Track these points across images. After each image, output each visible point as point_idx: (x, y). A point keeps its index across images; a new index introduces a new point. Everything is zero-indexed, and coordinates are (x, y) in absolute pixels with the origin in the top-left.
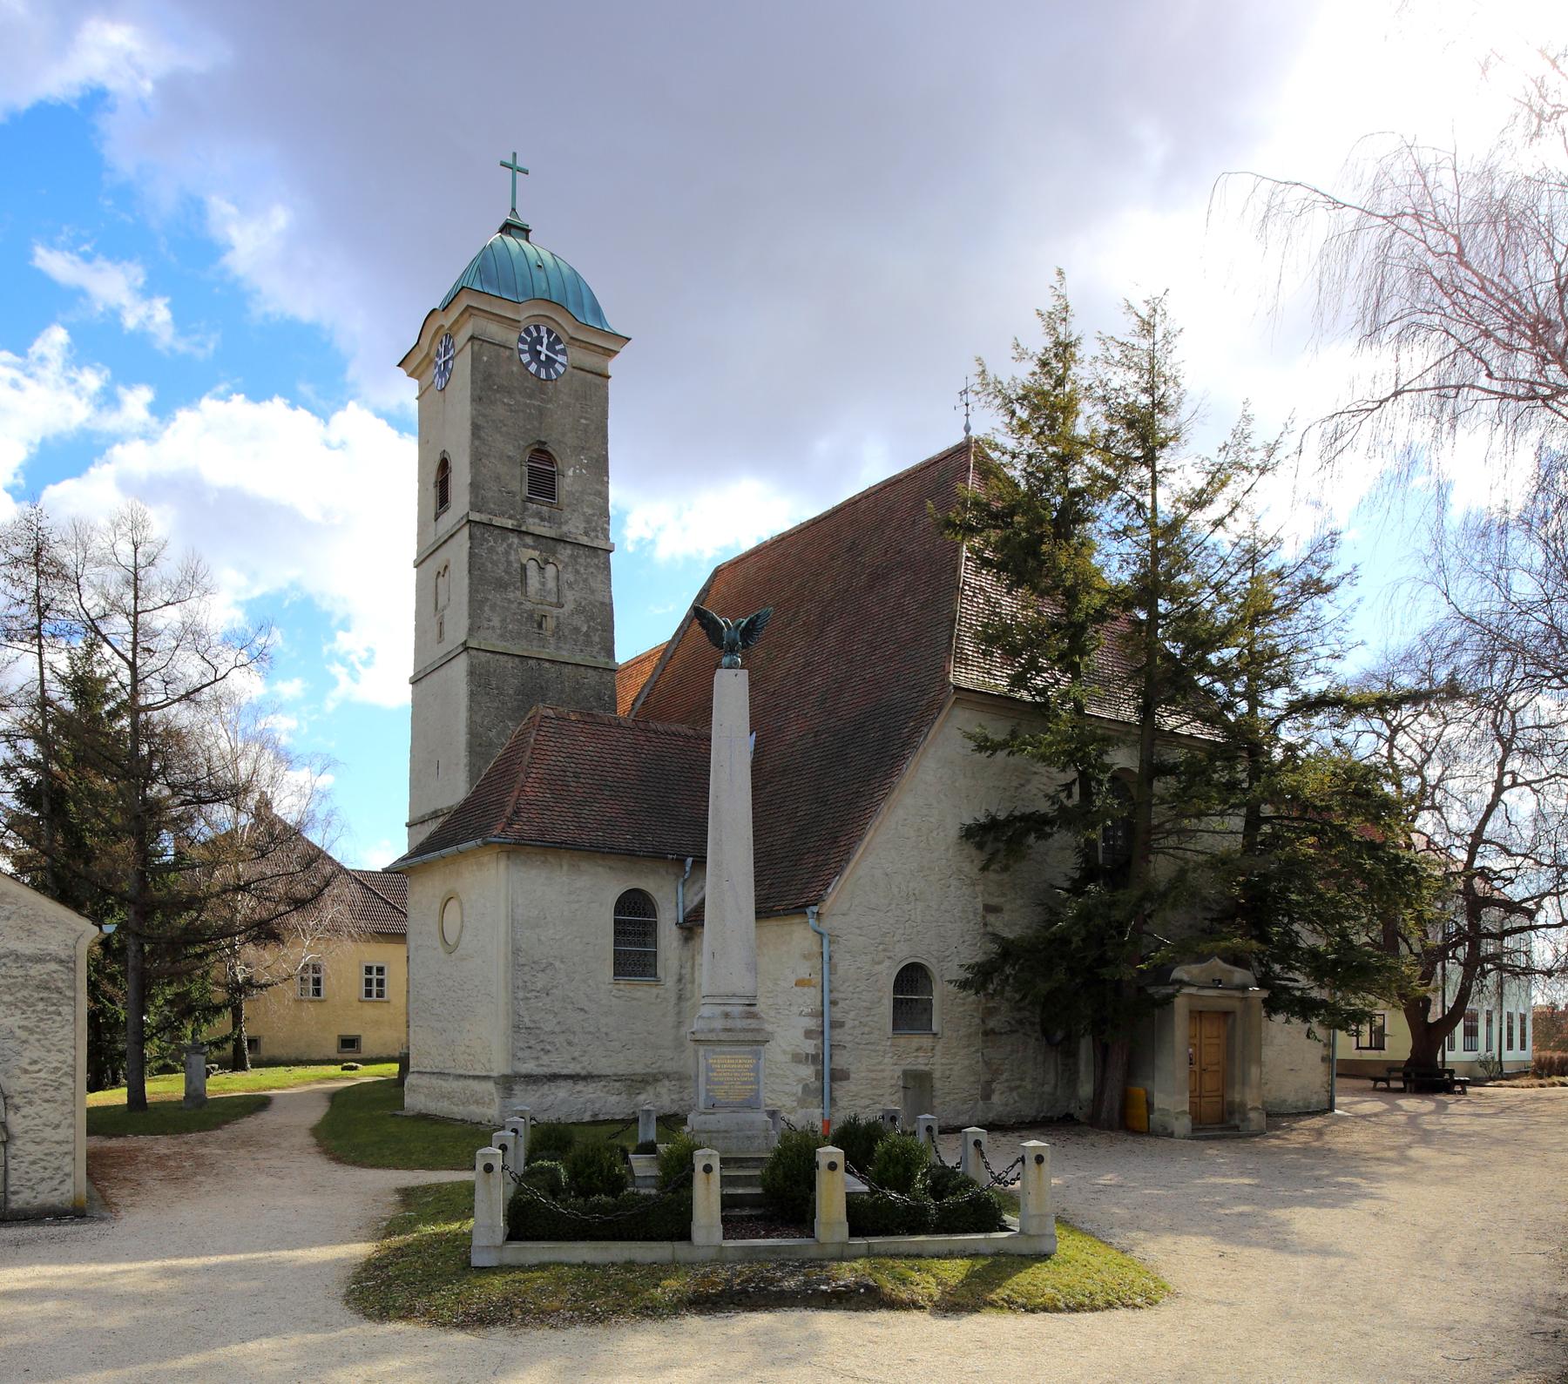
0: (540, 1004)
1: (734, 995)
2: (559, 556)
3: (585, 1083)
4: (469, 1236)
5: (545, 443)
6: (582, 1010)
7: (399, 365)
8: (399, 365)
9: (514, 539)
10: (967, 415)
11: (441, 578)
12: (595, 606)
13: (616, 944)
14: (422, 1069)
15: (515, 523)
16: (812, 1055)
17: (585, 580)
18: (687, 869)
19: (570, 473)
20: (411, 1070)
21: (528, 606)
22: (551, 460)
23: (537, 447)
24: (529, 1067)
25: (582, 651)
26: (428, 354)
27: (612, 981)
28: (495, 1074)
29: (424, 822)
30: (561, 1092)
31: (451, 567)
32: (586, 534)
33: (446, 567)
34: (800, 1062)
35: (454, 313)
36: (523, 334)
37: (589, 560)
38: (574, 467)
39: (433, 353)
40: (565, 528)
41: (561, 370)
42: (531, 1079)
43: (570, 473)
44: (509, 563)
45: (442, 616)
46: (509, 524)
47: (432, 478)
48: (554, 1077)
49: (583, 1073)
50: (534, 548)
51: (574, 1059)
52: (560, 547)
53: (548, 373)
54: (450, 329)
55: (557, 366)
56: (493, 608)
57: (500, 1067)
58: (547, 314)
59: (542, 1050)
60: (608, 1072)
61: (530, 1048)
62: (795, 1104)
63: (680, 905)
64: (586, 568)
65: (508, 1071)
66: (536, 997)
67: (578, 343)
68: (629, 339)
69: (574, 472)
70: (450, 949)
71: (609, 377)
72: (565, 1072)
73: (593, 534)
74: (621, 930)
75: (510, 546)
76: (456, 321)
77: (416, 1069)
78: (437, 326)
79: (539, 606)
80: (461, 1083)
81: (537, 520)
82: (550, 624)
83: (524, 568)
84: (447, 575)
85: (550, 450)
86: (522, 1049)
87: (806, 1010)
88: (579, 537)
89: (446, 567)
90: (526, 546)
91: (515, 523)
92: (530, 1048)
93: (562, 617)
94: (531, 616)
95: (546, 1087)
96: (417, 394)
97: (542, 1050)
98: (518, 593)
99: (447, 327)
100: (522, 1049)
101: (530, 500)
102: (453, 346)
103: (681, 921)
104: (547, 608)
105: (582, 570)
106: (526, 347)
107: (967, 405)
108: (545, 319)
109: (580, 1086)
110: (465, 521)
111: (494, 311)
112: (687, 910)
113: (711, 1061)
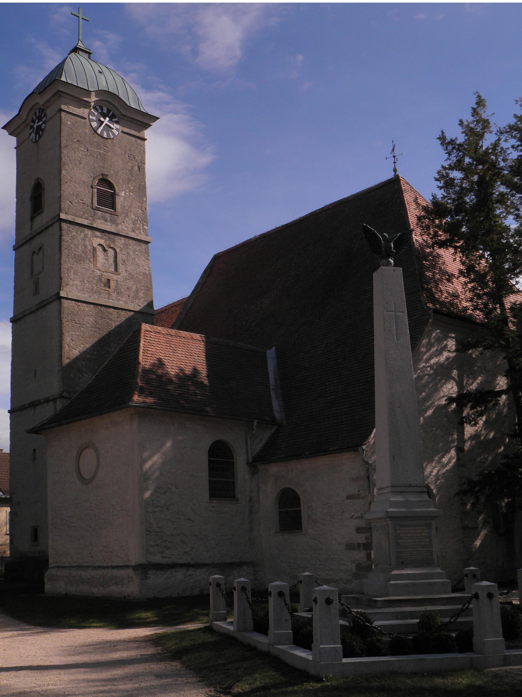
0: (163, 516)
1: (410, 486)
2: (117, 243)
3: (194, 569)
4: (471, 622)
5: (107, 175)
6: (190, 520)
7: (3, 128)
8: (3, 128)
9: (89, 232)
10: (395, 163)
11: (36, 256)
12: (140, 275)
13: (210, 476)
14: (60, 564)
15: (89, 222)
16: (363, 544)
17: (134, 259)
18: (255, 428)
19: (123, 194)
20: (50, 566)
21: (98, 273)
22: (110, 185)
23: (102, 177)
24: (156, 559)
25: (132, 302)
26: (25, 121)
27: (208, 500)
28: (133, 563)
29: (24, 409)
30: (179, 575)
31: (495, 114)
32: (133, 231)
33: (40, 248)
34: (354, 549)
35: (48, 95)
36: (92, 110)
37: (135, 247)
38: (125, 191)
39: (29, 119)
40: (120, 227)
41: (116, 133)
42: (159, 567)
43: (123, 194)
44: (85, 246)
45: (38, 279)
46: (86, 222)
47: (28, 195)
48: (173, 566)
49: (192, 562)
50: (101, 238)
51: (186, 553)
52: (117, 238)
53: (108, 134)
54: (43, 105)
55: (114, 131)
56: (76, 273)
57: (135, 558)
58: (108, 100)
59: (165, 547)
60: (208, 561)
61: (157, 545)
62: (350, 577)
63: (249, 451)
64: (134, 251)
65: (143, 561)
66: (160, 511)
67: (126, 118)
68: (158, 118)
69: (125, 193)
70: (85, 481)
71: (145, 140)
72: (181, 561)
73: (137, 232)
74: (213, 468)
75: (86, 236)
76: (49, 100)
77: (55, 565)
78: (32, 104)
79: (105, 273)
80: (100, 572)
81: (102, 221)
82: (113, 284)
83: (94, 249)
84: (41, 253)
85: (110, 179)
86: (152, 546)
87: (356, 515)
88: (130, 233)
89: (40, 248)
90: (97, 237)
91: (89, 222)
92: (157, 545)
93: (119, 280)
94: (100, 280)
95: (169, 571)
96: (16, 146)
97: (165, 547)
98: (92, 265)
99: (41, 103)
100: (152, 546)
101: (98, 209)
102: (45, 115)
103: (250, 461)
104: (110, 275)
105: (131, 253)
106: (94, 118)
107: (394, 157)
108: (107, 103)
109: (191, 571)
110: (57, 219)
111: (75, 95)
112: (254, 454)
113: (398, 532)
